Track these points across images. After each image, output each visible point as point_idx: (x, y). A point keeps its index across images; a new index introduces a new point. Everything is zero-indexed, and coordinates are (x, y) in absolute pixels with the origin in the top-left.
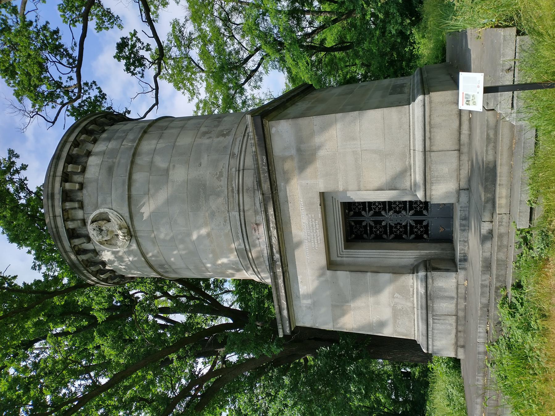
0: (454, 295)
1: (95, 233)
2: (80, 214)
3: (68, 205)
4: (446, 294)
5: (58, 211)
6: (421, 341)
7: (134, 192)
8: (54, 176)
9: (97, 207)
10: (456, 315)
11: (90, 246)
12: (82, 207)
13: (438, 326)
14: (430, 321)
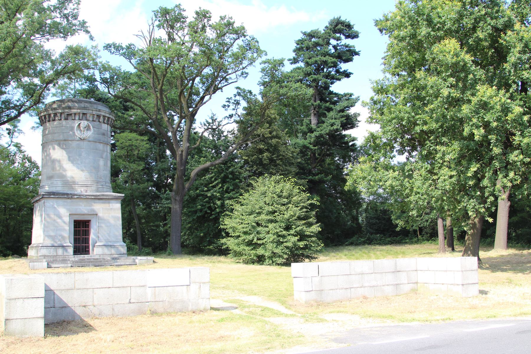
0: (65, 254)
1: (85, 125)
2: (91, 119)
3: (95, 116)
4: (65, 252)
5: (94, 113)
6: (31, 245)
7: (98, 144)
8: (105, 113)
9: (93, 127)
10: (57, 256)
11: (77, 118)
12: (93, 121)
13: (52, 250)
14: (53, 248)
